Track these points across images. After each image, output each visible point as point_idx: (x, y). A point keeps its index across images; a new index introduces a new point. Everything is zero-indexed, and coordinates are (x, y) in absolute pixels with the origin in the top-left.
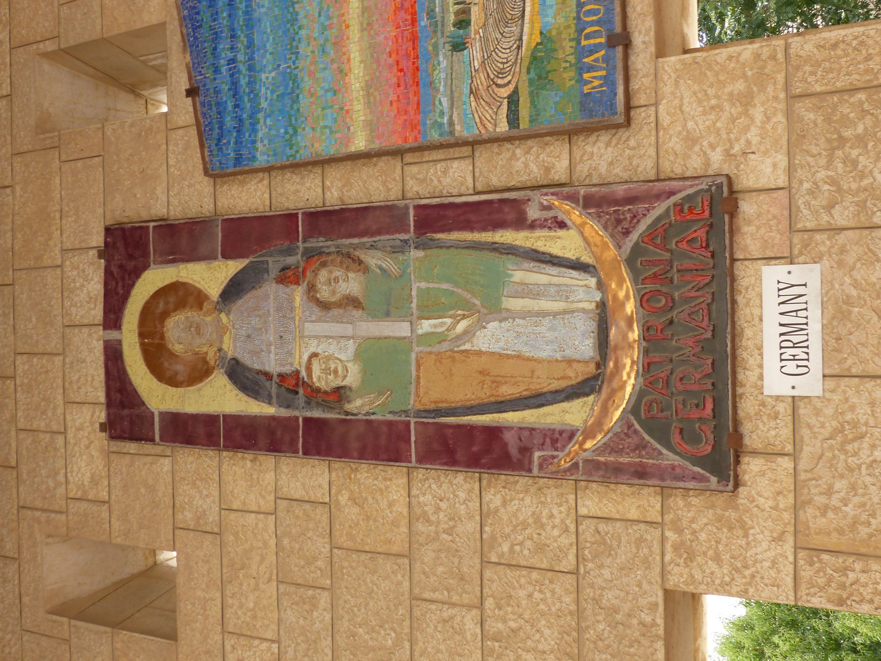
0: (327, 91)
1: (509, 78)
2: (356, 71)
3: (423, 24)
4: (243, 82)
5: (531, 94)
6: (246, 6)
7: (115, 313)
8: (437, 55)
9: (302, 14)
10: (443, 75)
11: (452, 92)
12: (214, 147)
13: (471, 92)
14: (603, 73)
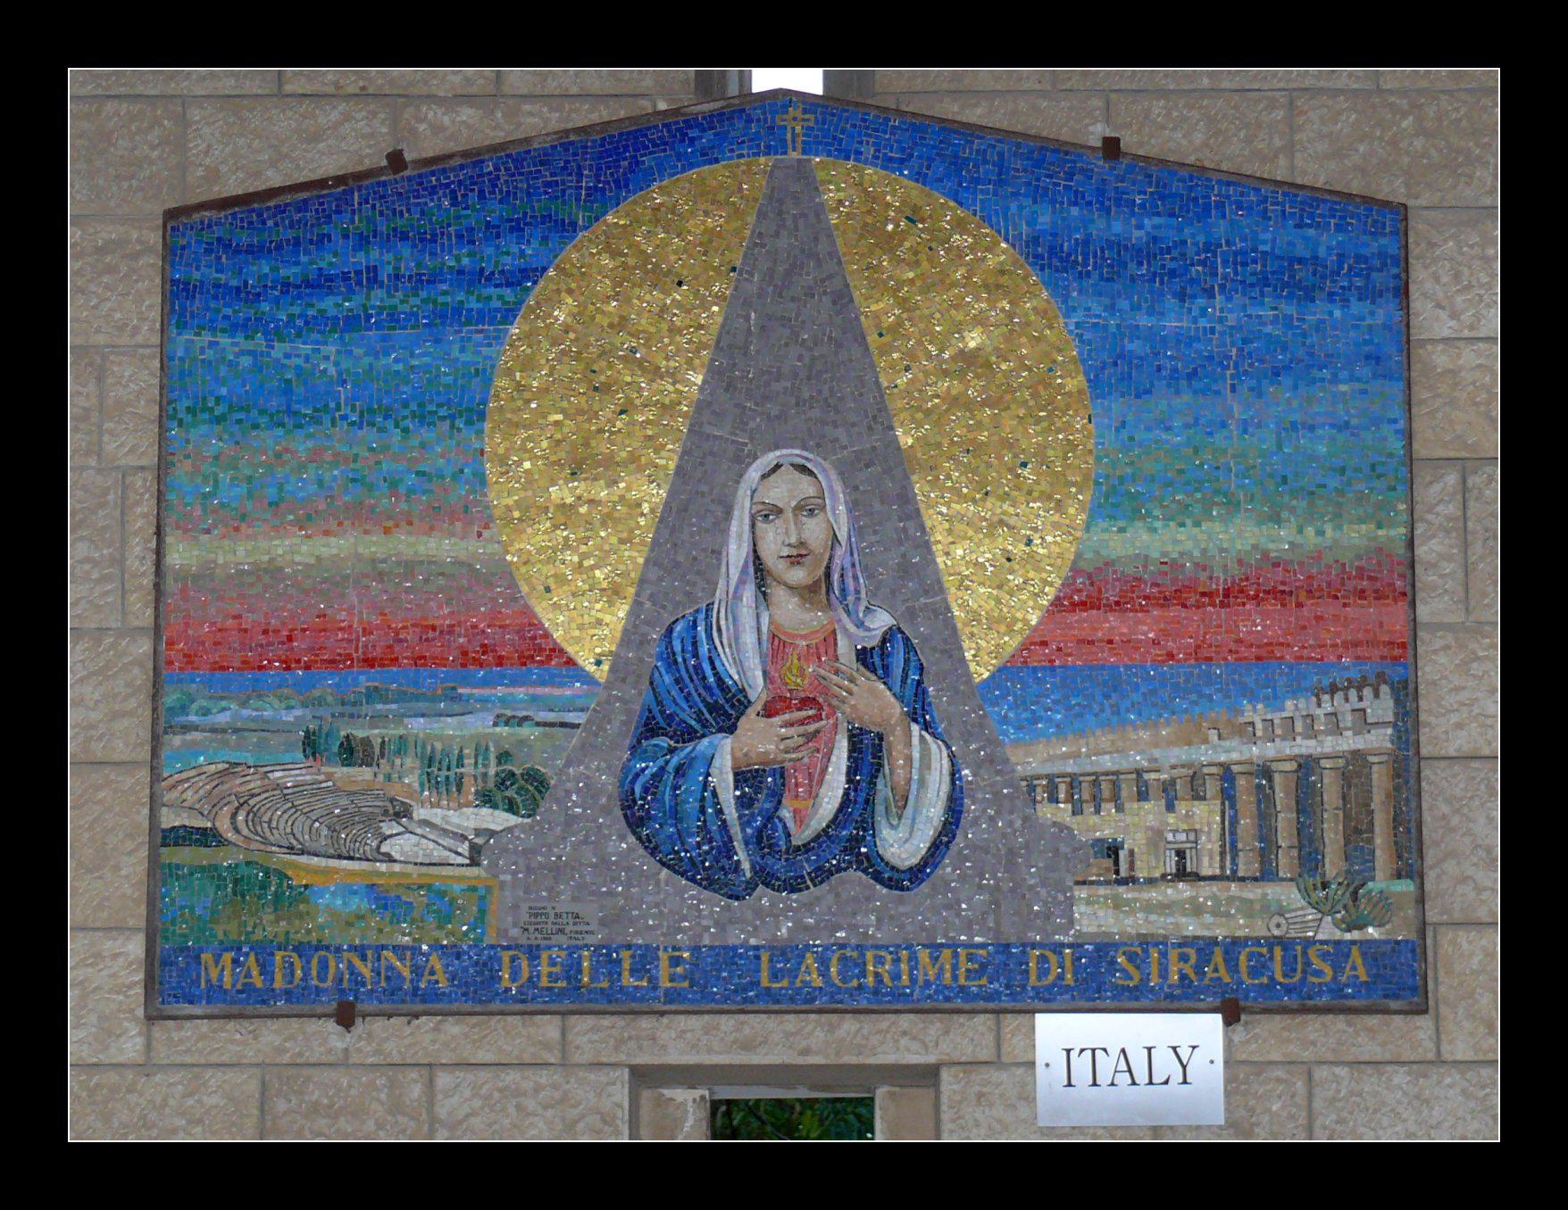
0: (281, 488)
1: (245, 831)
3: (362, 678)
4: (328, 304)
8: (304, 705)
9: (428, 434)
12: (218, 232)
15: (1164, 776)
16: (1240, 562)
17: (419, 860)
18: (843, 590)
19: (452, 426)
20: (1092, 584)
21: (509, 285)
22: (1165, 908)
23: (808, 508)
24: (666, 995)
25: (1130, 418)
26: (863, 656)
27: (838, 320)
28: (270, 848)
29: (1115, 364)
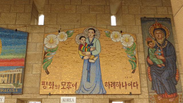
22: (2, 85)
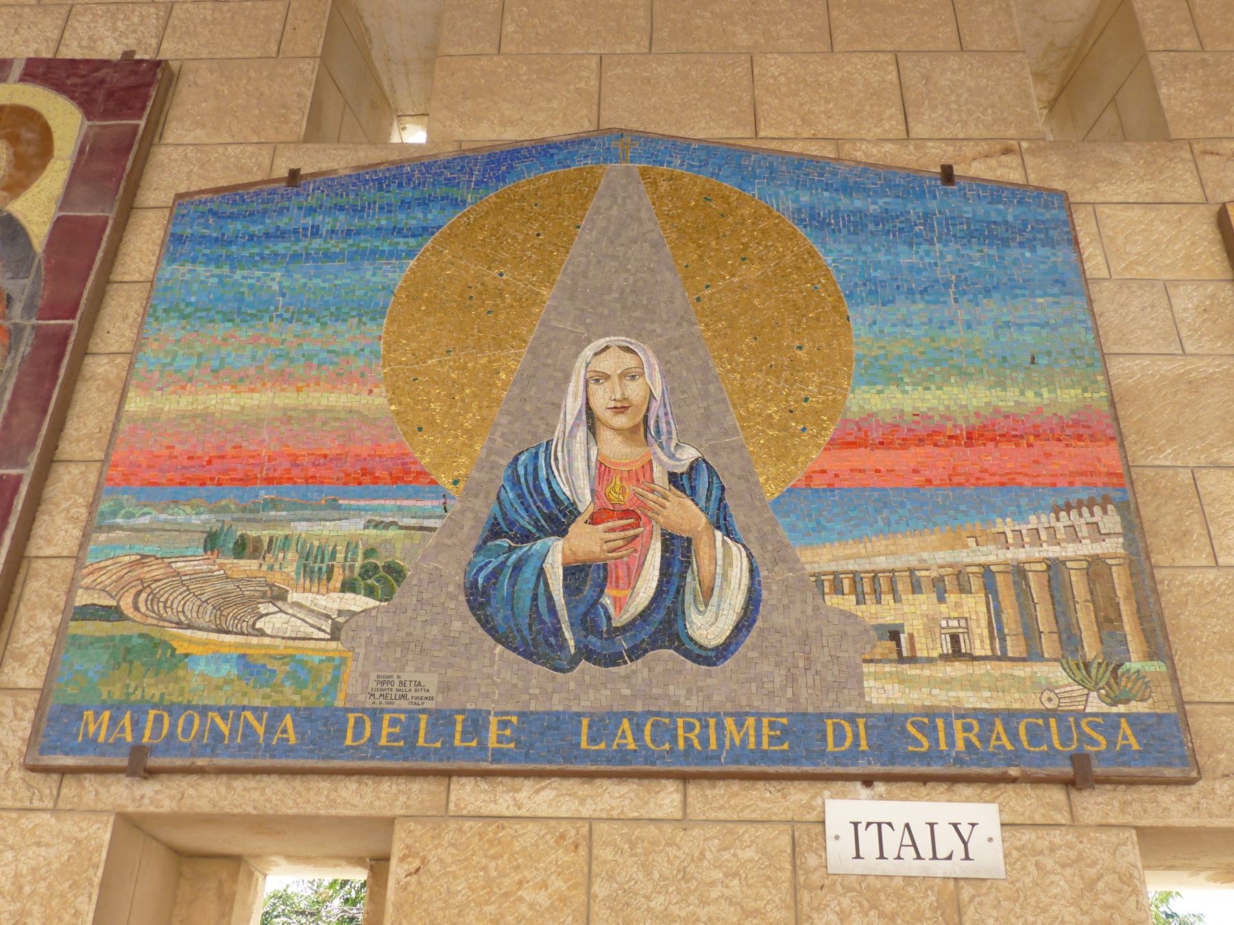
0: (222, 360)
1: (143, 609)
2: (233, 400)
3: (262, 493)
4: (281, 247)
5: (112, 638)
6: (383, 252)
7: (44, 74)
8: (211, 512)
9: (341, 327)
10: (181, 518)
11: (153, 530)
13: (144, 557)
14: (101, 739)
15: (934, 574)
16: (977, 415)
17: (287, 635)
18: (658, 432)
19: (360, 321)
20: (860, 429)
21: (413, 236)
22: (947, 683)
23: (629, 375)
24: (493, 755)
25: (879, 318)
26: (674, 478)
27: (655, 258)
28: (161, 623)
29: (865, 284)
